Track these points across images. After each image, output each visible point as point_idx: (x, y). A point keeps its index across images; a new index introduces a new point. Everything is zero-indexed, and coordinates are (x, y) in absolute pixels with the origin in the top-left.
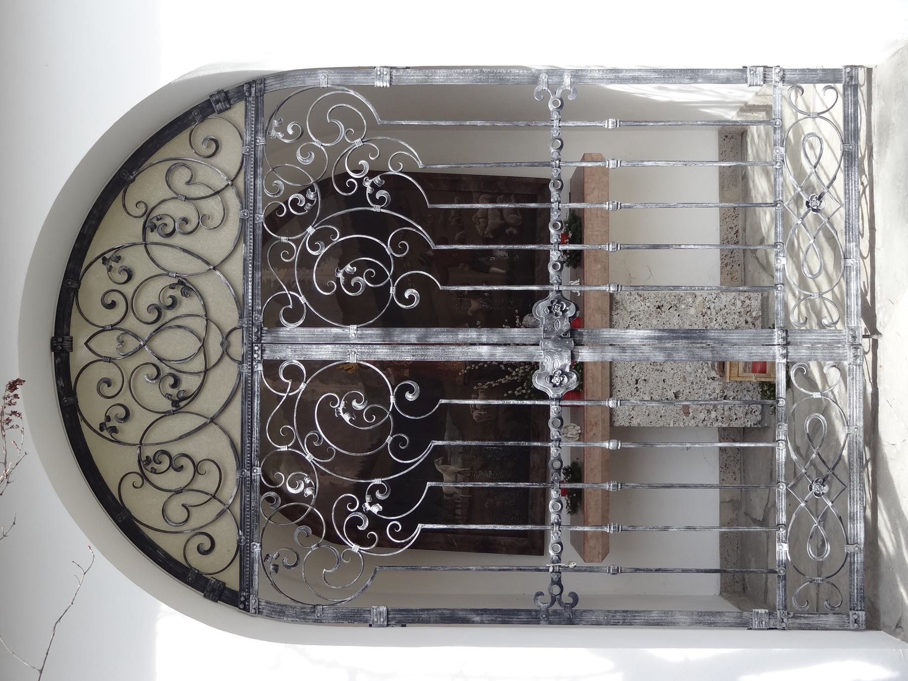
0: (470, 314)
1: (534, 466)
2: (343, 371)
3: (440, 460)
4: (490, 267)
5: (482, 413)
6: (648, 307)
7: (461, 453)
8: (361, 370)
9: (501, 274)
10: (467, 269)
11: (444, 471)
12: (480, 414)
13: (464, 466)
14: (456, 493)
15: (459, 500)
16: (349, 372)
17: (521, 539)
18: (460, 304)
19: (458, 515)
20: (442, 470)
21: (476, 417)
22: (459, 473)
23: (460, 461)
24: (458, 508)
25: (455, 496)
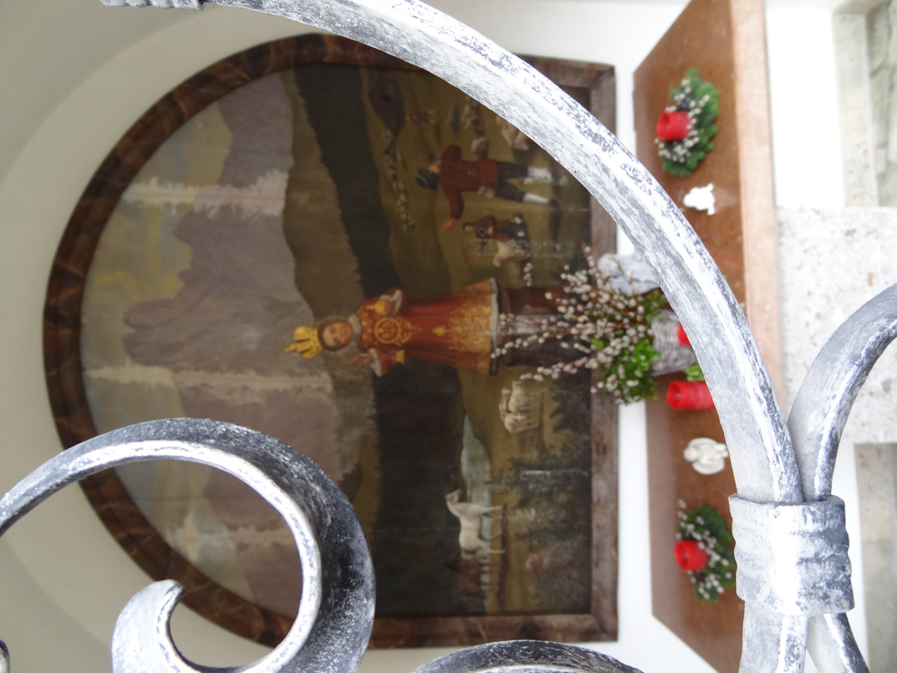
0: (497, 263)
1: (599, 500)
2: (295, 355)
3: (455, 495)
4: (523, 193)
5: (520, 417)
6: (832, 232)
7: (488, 483)
8: (326, 352)
9: (542, 205)
10: (490, 194)
11: (462, 512)
12: (516, 420)
13: (493, 502)
14: (480, 548)
15: (485, 558)
16: (307, 355)
17: (581, 617)
18: (482, 249)
19: (485, 584)
20: (459, 511)
21: (511, 424)
22: (486, 515)
23: (486, 495)
24: (484, 572)
25: (479, 553)
